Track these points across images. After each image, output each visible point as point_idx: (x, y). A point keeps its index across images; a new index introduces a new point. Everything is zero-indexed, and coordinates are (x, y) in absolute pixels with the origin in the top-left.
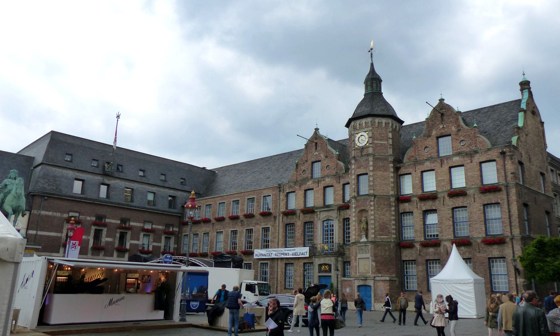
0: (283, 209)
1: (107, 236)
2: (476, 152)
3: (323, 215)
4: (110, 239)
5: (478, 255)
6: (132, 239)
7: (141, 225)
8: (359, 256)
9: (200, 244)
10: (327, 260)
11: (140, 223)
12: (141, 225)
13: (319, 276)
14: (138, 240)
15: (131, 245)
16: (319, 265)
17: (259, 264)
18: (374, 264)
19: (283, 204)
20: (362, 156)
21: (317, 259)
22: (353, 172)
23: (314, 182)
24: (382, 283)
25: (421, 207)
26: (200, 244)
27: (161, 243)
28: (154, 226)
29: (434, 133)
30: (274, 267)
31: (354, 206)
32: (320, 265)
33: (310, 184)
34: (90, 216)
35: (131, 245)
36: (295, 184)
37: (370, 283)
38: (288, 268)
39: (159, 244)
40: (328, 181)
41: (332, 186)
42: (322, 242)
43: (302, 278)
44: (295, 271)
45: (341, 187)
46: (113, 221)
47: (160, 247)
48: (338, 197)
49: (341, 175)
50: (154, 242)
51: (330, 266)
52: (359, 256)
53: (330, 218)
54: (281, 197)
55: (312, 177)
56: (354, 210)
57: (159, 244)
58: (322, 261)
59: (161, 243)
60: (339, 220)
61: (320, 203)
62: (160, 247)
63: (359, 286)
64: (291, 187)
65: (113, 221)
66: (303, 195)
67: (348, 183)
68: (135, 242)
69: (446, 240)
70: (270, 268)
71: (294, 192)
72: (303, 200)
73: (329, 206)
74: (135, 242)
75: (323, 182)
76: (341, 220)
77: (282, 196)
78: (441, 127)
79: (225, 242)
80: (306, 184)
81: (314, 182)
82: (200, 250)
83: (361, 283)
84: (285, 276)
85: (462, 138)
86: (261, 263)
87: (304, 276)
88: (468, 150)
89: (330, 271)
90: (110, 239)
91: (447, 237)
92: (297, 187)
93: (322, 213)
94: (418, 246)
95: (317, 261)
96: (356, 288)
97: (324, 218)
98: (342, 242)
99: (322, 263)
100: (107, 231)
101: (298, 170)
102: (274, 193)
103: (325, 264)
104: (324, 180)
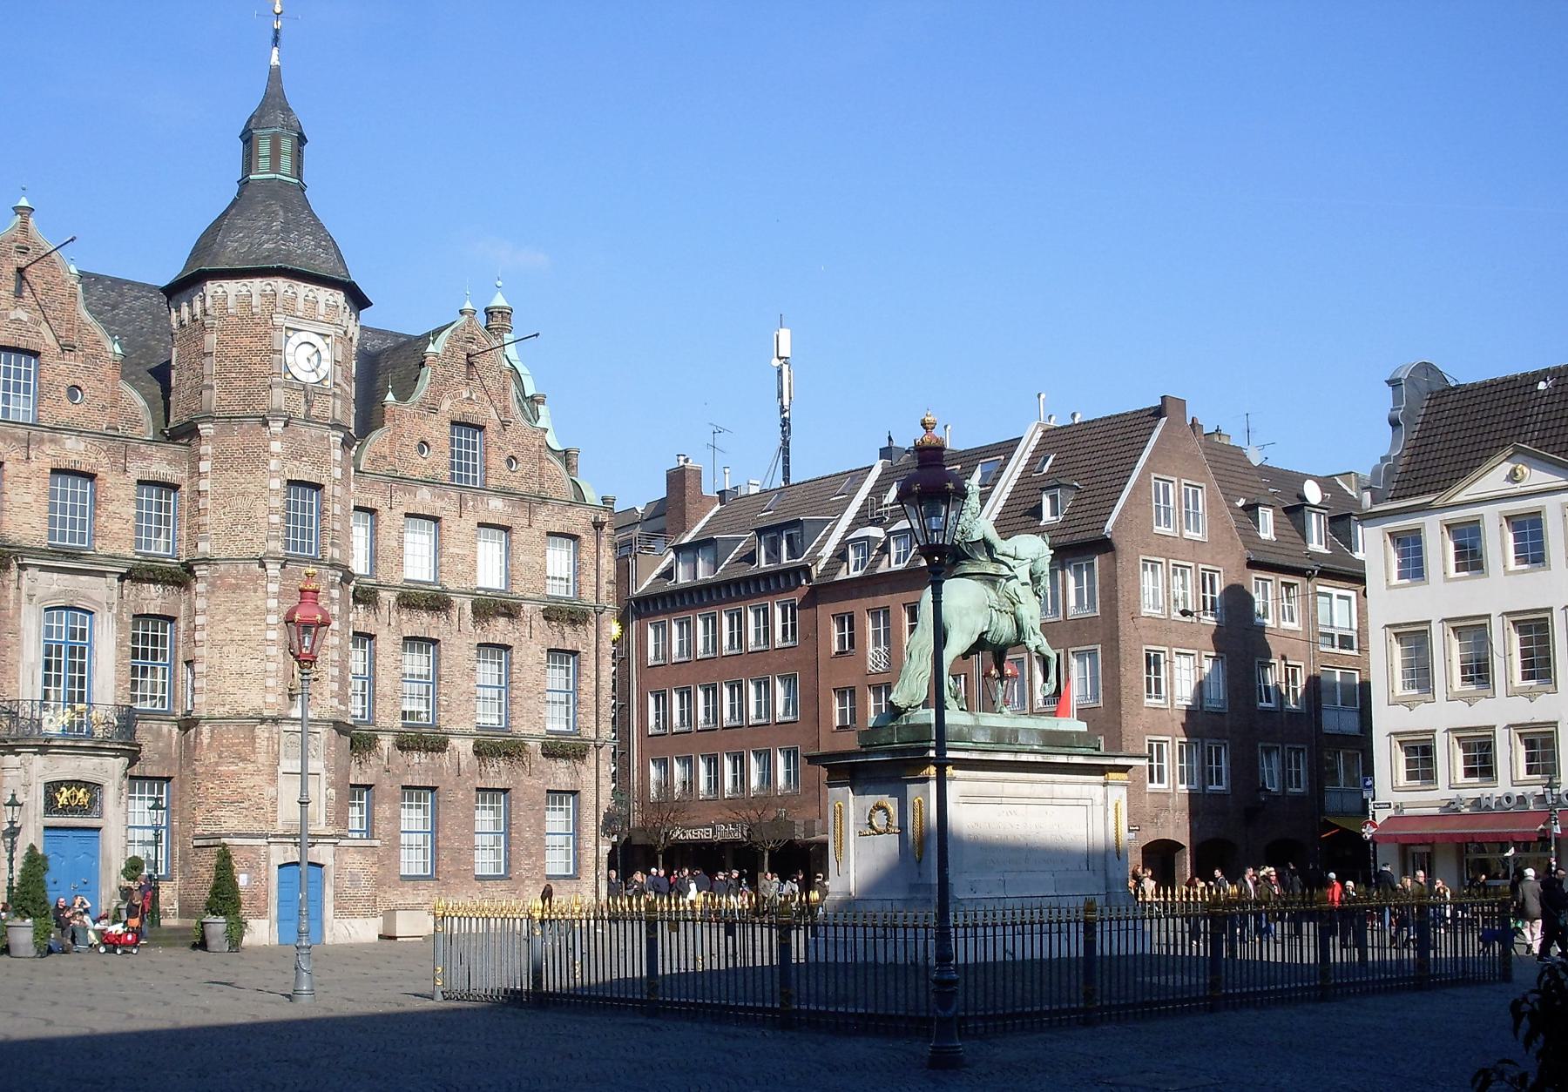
2: (544, 501)
3: (52, 585)
5: (528, 781)
13: (46, 828)
18: (332, 791)
20: (308, 419)
22: (274, 464)
24: (358, 857)
25: (399, 623)
29: (446, 405)
31: (273, 588)
32: (52, 788)
37: (322, 853)
51: (93, 788)
56: (272, 603)
60: (119, 620)
63: (280, 867)
69: (463, 734)
78: (466, 395)
83: (293, 855)
85: (511, 450)
88: (523, 489)
89: (93, 805)
91: (462, 725)
94: (386, 742)
96: (275, 871)
97: (55, 596)
103: (70, 784)
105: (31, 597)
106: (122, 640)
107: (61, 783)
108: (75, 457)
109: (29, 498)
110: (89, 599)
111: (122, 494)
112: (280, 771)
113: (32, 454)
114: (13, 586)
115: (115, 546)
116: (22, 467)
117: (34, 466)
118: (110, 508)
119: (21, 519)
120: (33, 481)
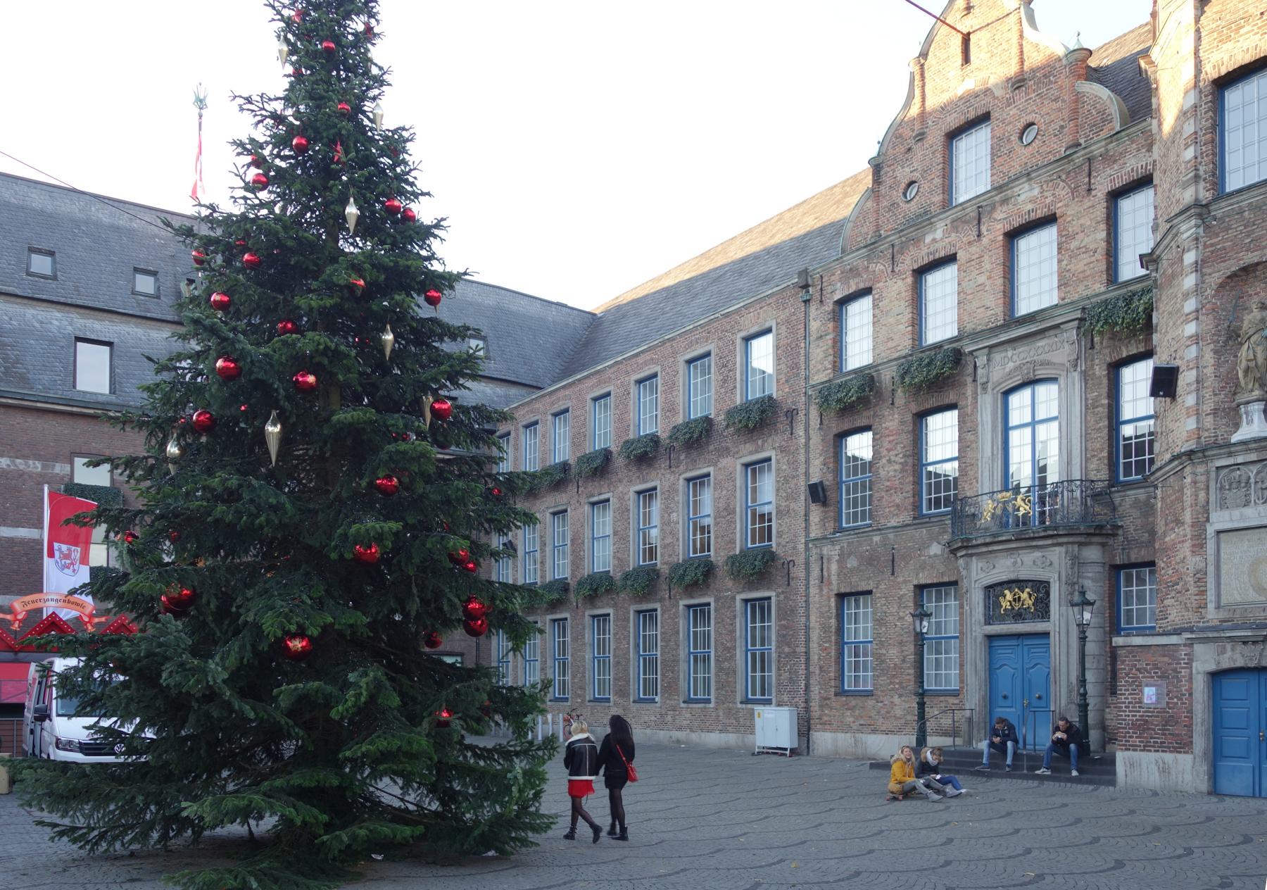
0: (821, 373)
3: (1004, 365)
8: (1220, 520)
9: (543, 551)
10: (1028, 564)
16: (989, 588)
17: (738, 604)
19: (819, 353)
21: (976, 565)
23: (955, 225)
26: (543, 551)
30: (793, 611)
33: (938, 238)
36: (869, 258)
38: (850, 610)
40: (1028, 199)
41: (1049, 220)
42: (998, 487)
43: (911, 648)
44: (879, 622)
45: (1101, 211)
48: (1079, 265)
49: (1097, 149)
52: (1220, 520)
53: (1041, 373)
54: (814, 326)
55: (947, 204)
58: (1003, 568)
61: (990, 309)
64: (853, 272)
66: (907, 295)
67: (1145, 181)
70: (779, 618)
71: (867, 292)
72: (907, 316)
73: (1031, 318)
75: (999, 214)
76: (1100, 371)
77: (818, 321)
79: (620, 536)
80: (917, 241)
81: (955, 225)
82: (543, 571)
84: (841, 644)
86: (746, 601)
87: (920, 638)
92: (879, 267)
93: (997, 357)
95: (980, 573)
98: (1104, 474)
99: (1004, 578)
101: (883, 189)
102: (783, 315)
104: (1005, 201)
105: (984, 385)
106: (1095, 400)
107: (1001, 584)
108: (1030, 207)
109: (982, 279)
110: (1048, 363)
111: (1086, 221)
112: (1211, 530)
113: (984, 228)
114: (969, 379)
115: (1081, 288)
116: (973, 249)
117: (985, 241)
118: (1074, 244)
119: (975, 304)
120: (986, 257)
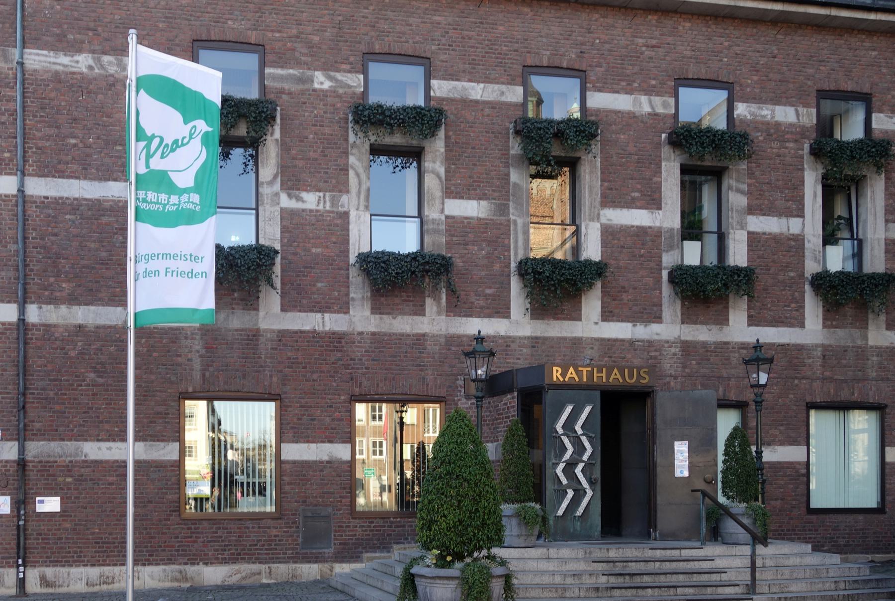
1: (451, 192)
4: (470, 209)
6: (610, 200)
7: (661, 105)
11: (648, 91)
12: (661, 105)
14: (653, 201)
15: (609, 234)
27: (800, 214)
28: (742, 109)
34: (326, 68)
35: (609, 234)
39: (794, 226)
46: (477, 91)
47: (798, 242)
50: (752, 210)
57: (794, 226)
59: (800, 213)
62: (798, 242)
65: (477, 91)
68: (638, 217)
74: (638, 217)
90: (470, 209)
100: (450, 159)
